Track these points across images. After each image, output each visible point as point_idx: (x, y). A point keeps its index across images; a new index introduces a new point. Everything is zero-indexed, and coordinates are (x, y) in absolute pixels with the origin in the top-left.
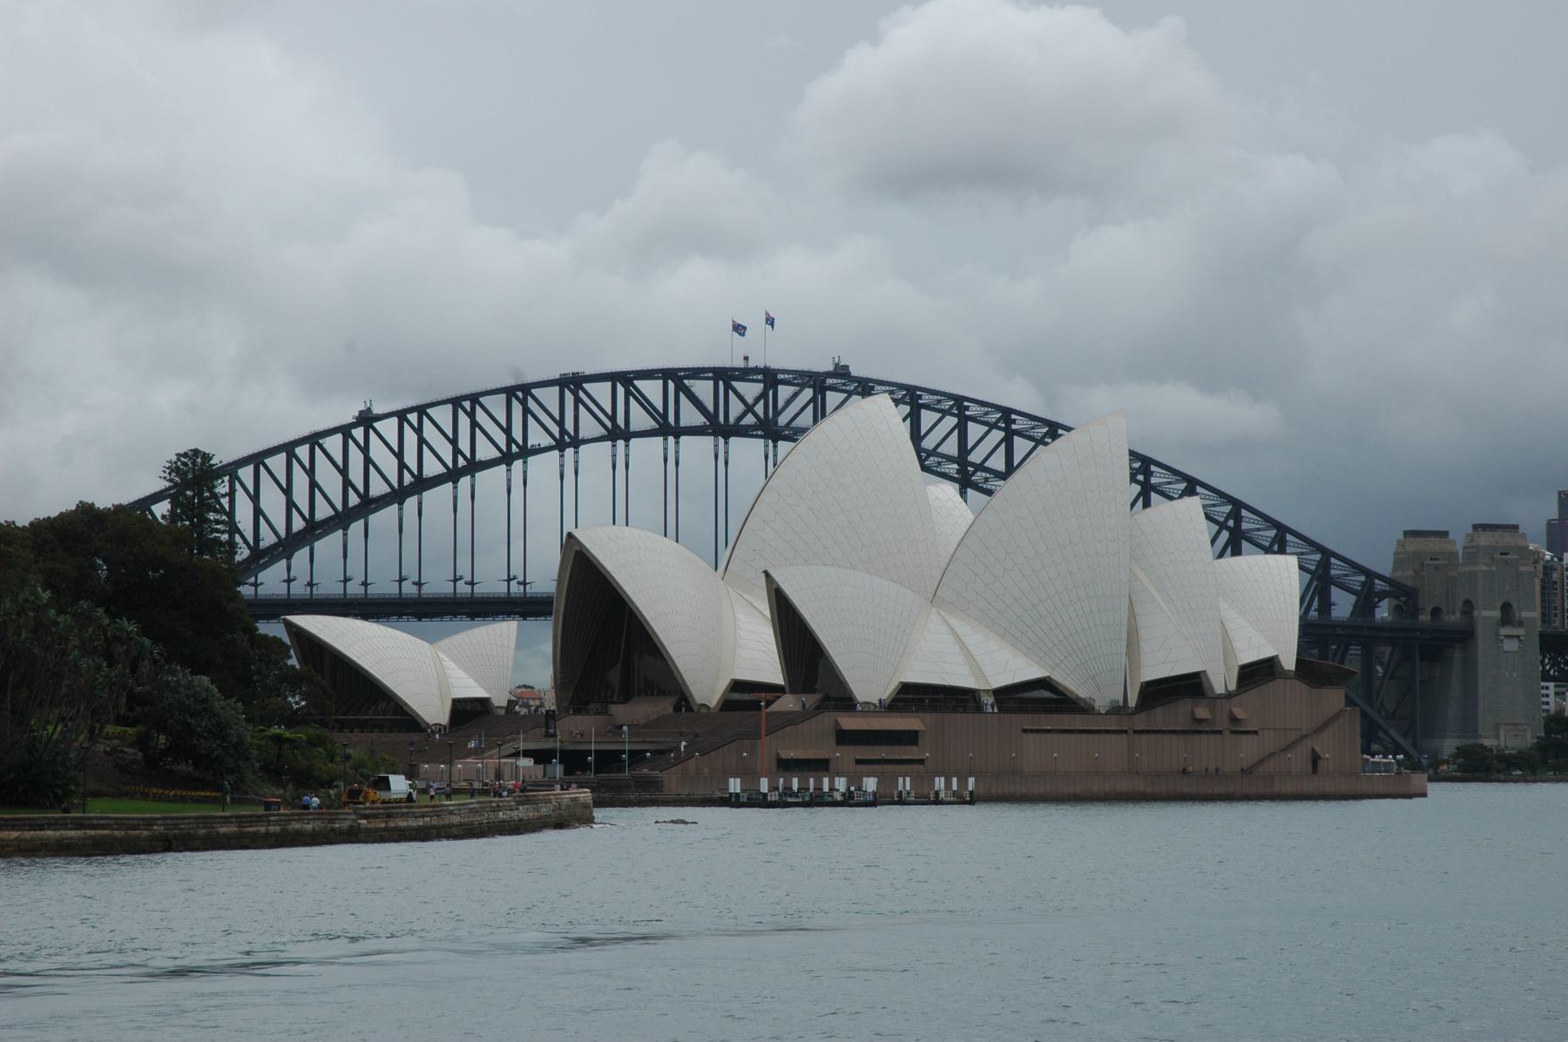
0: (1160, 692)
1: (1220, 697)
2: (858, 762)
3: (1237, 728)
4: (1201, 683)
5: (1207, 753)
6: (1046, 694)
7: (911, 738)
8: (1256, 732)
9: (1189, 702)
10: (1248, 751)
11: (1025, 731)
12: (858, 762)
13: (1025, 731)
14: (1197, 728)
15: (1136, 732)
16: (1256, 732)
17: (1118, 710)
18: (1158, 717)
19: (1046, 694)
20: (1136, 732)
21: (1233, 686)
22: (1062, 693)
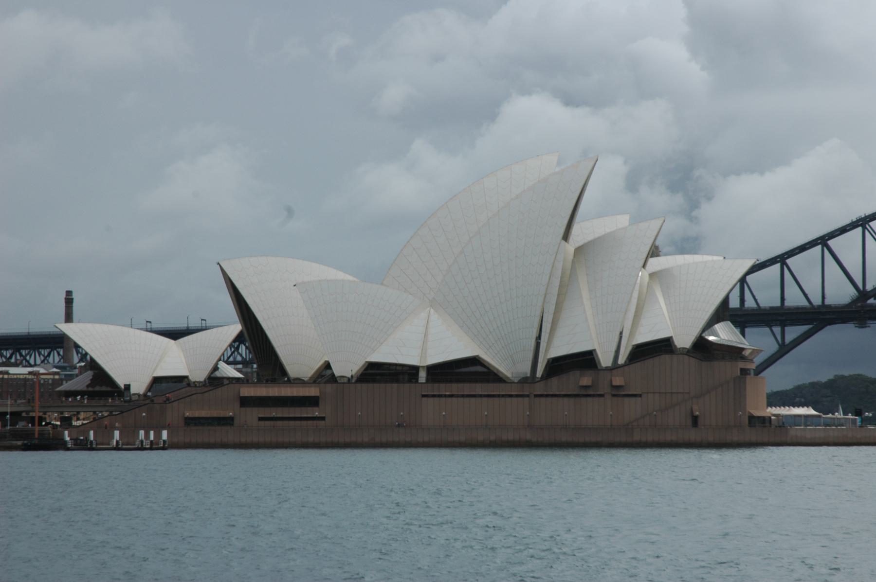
0: (561, 366)
1: (607, 369)
2: (260, 419)
3: (617, 392)
4: (593, 359)
5: (594, 412)
6: (479, 369)
7: (313, 401)
8: (640, 396)
9: (577, 373)
10: (631, 409)
11: (424, 396)
12: (260, 419)
13: (424, 396)
14: (585, 393)
15: (536, 396)
16: (640, 396)
17: (528, 380)
18: (555, 385)
19: (479, 369)
20: (536, 396)
21: (621, 360)
22: (488, 368)
